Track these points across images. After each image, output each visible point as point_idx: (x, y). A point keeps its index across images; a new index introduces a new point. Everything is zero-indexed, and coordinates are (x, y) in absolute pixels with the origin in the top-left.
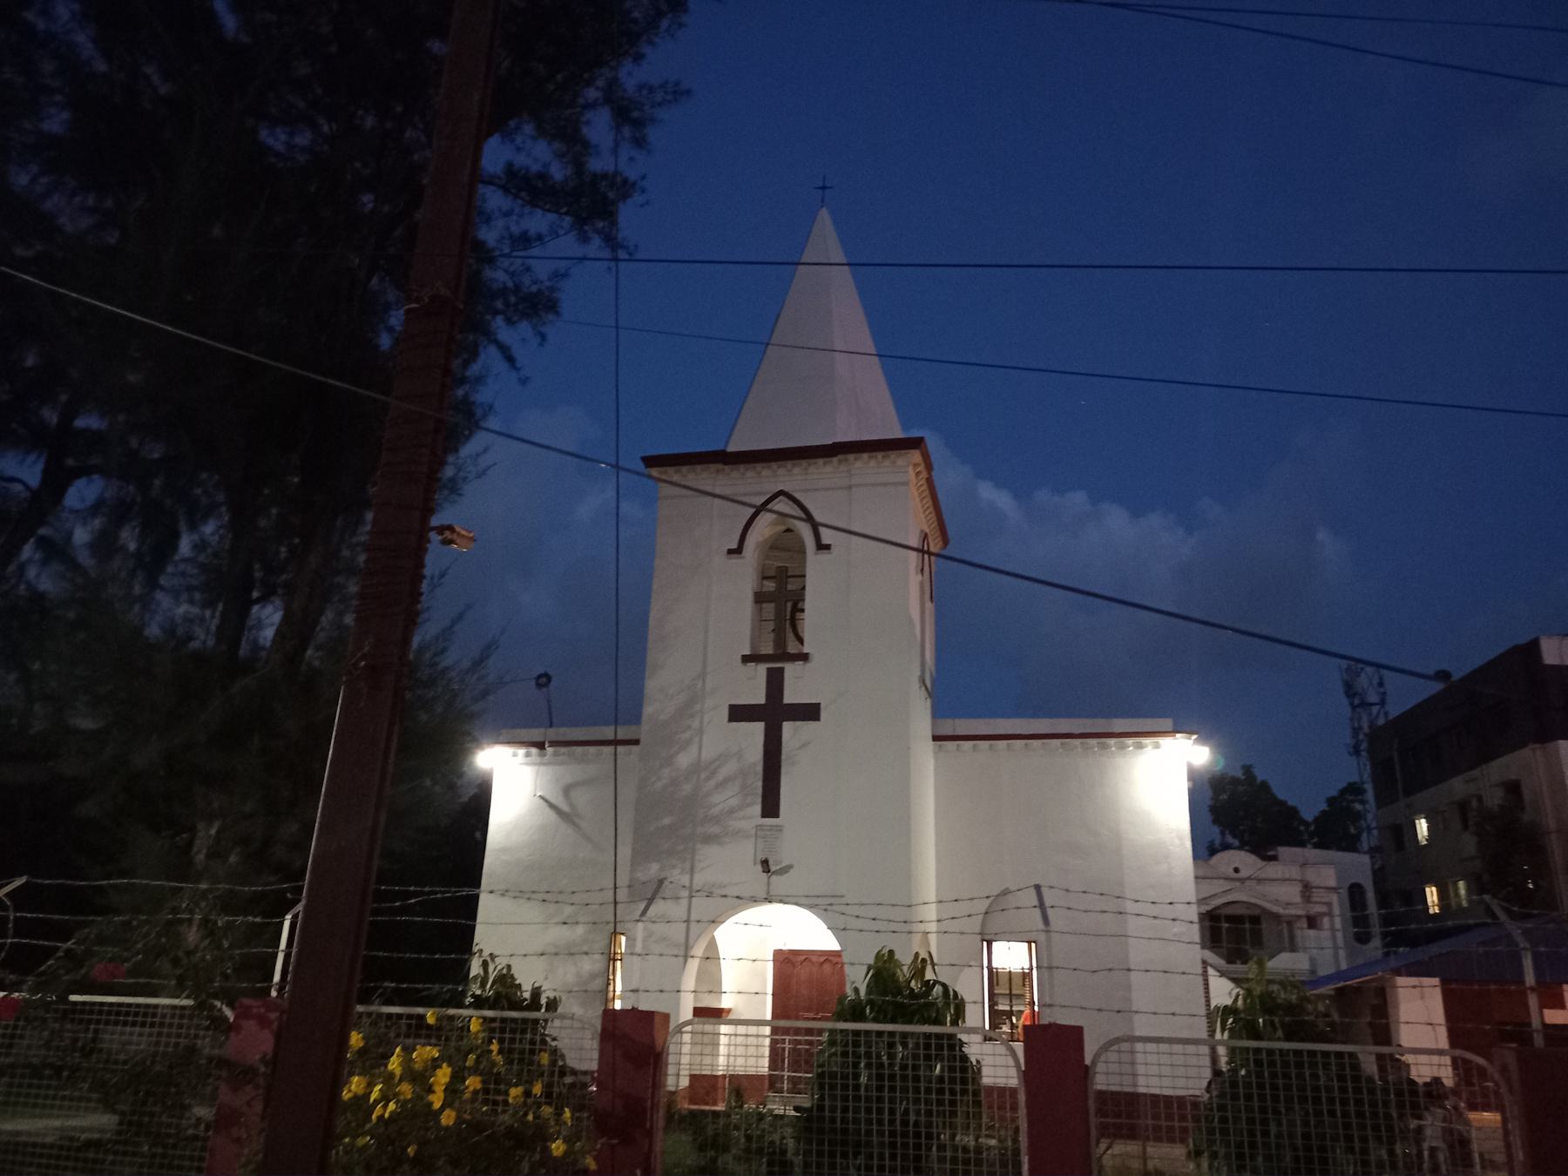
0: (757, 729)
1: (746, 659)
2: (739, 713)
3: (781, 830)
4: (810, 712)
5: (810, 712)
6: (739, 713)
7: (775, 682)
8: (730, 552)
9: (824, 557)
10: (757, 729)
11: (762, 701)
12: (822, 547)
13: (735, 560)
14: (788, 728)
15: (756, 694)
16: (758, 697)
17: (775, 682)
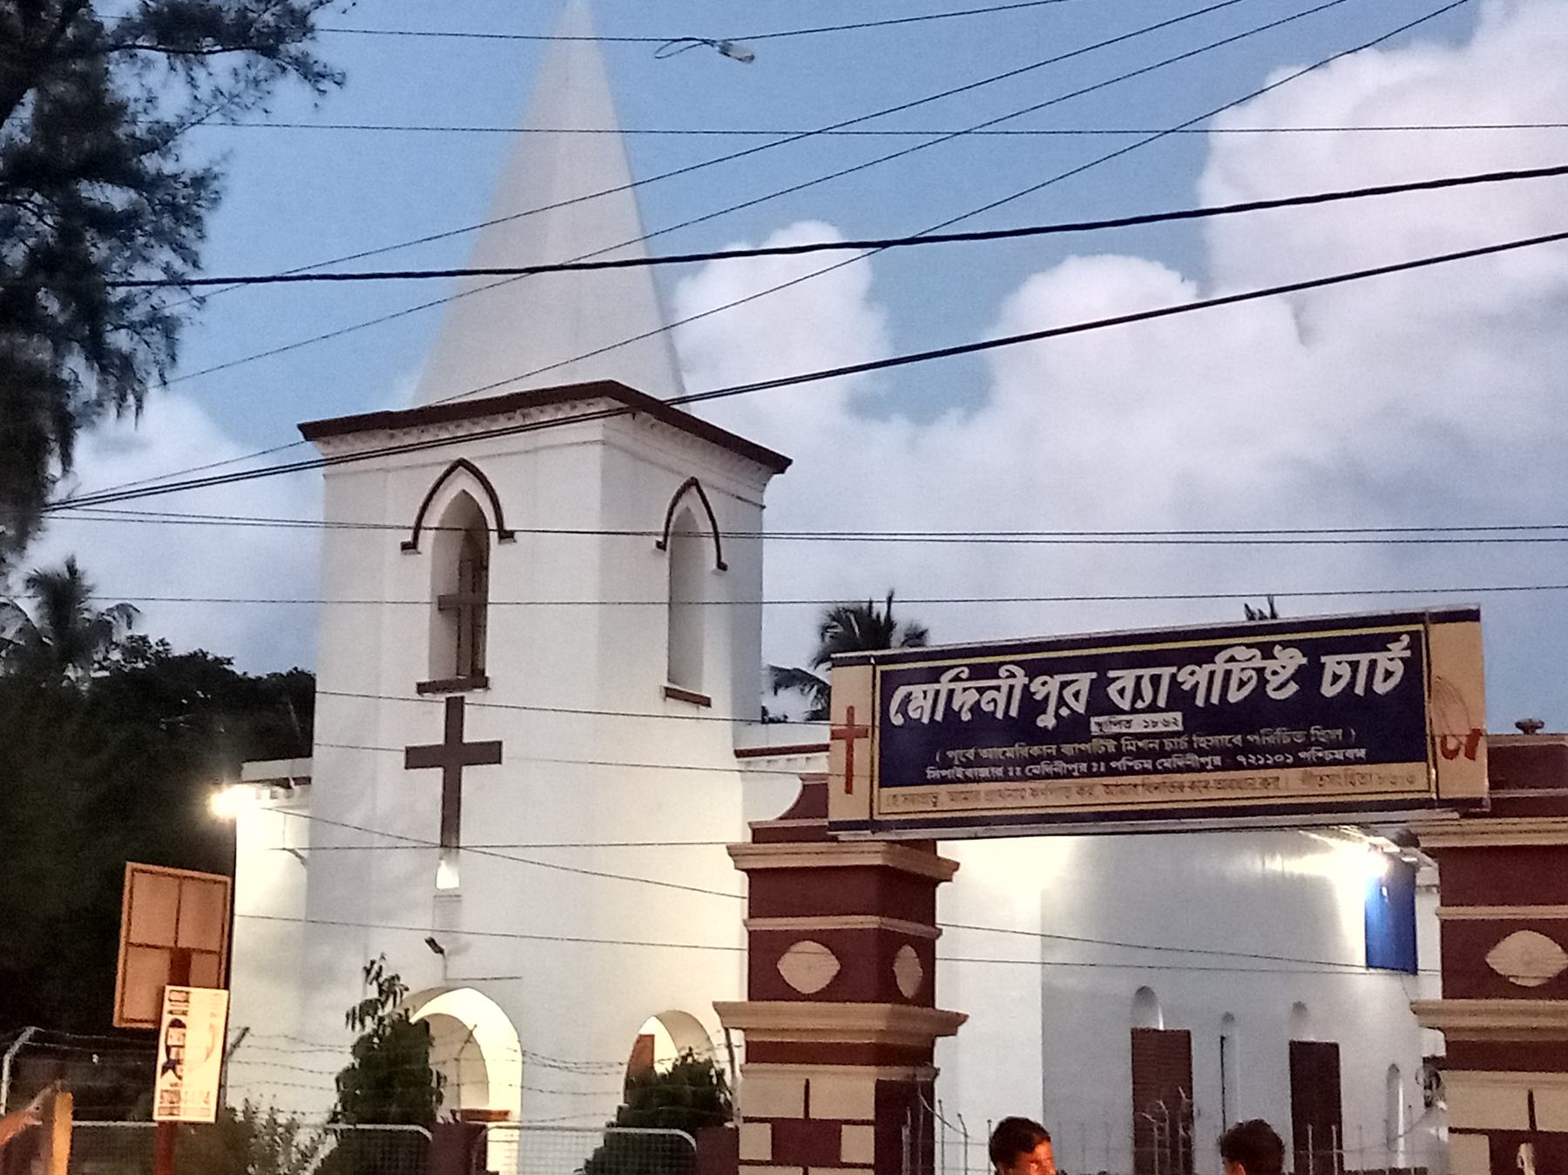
0: (437, 774)
1: (422, 688)
2: (417, 758)
3: (460, 901)
4: (490, 753)
5: (490, 753)
6: (417, 758)
7: (455, 713)
8: (405, 546)
9: (508, 547)
10: (437, 774)
11: (441, 742)
12: (506, 536)
13: (411, 558)
14: (470, 775)
15: (435, 735)
16: (435, 735)
17: (455, 713)
